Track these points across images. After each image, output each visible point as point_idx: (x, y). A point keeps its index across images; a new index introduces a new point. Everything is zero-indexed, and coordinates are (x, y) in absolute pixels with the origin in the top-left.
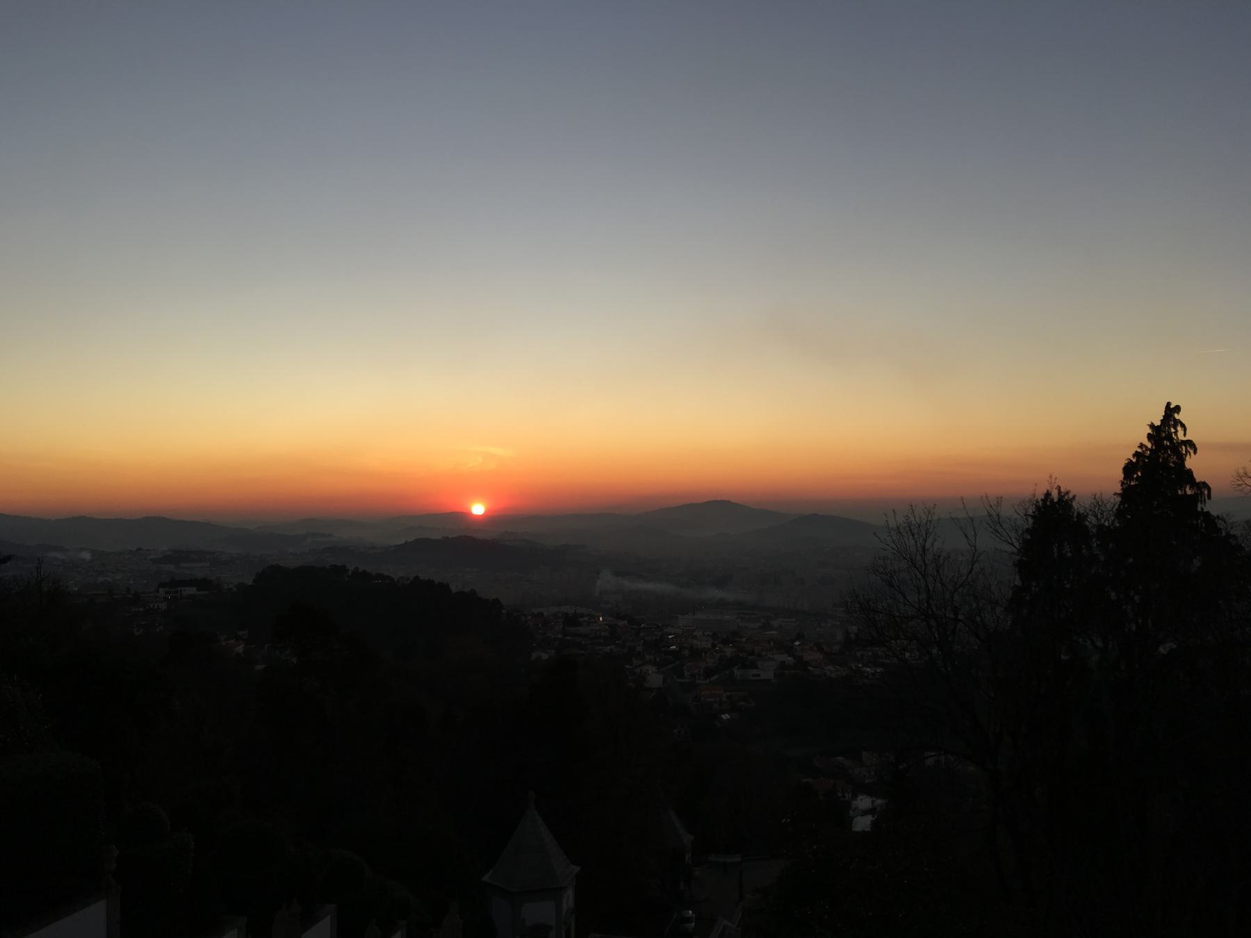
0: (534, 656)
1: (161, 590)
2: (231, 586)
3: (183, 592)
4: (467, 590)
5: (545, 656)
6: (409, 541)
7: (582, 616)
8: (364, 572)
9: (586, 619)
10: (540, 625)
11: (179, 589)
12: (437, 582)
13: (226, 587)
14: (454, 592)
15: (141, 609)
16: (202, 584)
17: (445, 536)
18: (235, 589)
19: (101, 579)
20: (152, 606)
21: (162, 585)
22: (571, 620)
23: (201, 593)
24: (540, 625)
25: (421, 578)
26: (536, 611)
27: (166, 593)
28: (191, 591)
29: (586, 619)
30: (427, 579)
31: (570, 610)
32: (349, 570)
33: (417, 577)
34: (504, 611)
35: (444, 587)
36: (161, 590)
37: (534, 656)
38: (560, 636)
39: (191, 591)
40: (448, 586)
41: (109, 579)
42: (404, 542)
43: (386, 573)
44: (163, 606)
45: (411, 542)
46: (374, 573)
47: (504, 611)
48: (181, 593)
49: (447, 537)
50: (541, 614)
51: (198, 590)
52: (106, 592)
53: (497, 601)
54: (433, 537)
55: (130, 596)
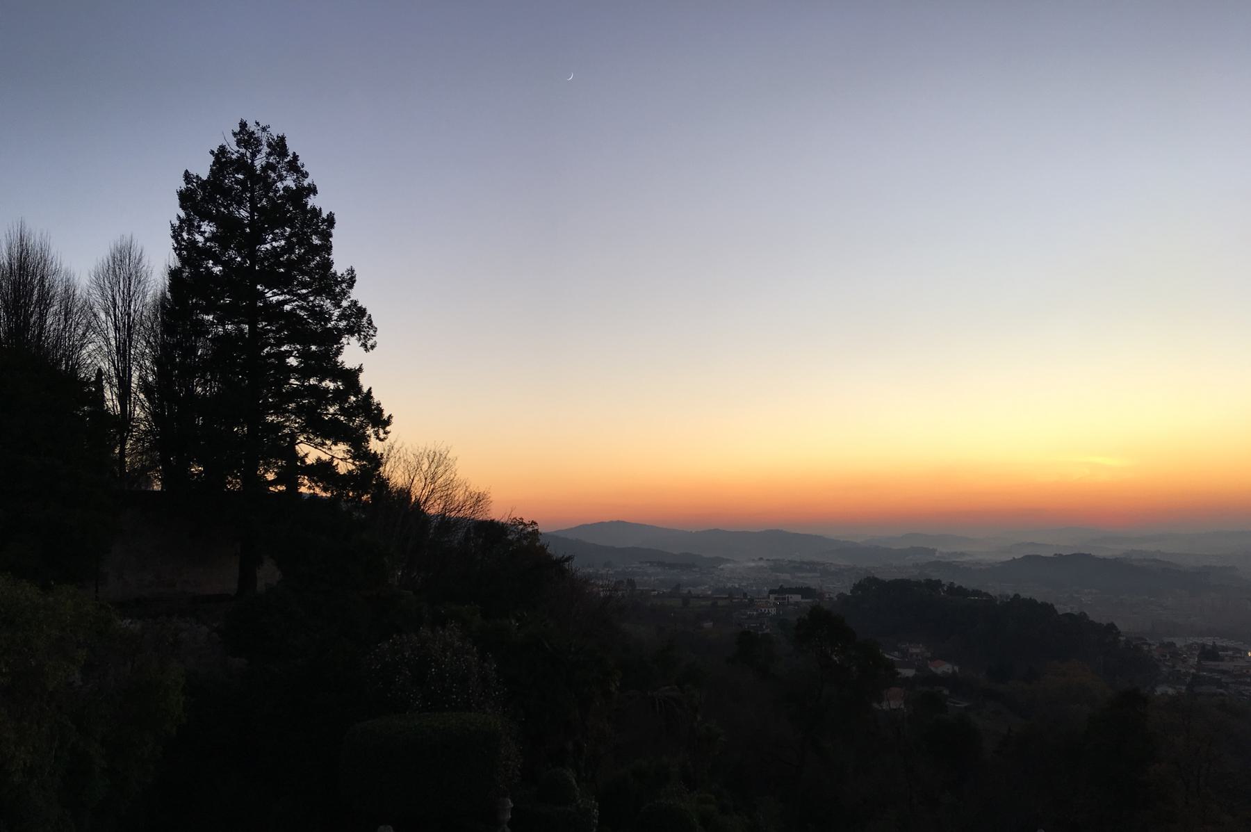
0: (1159, 690)
1: (771, 595)
2: (832, 595)
3: (790, 600)
4: (1076, 611)
5: (1171, 691)
6: (1016, 557)
7: (1225, 649)
8: (960, 587)
9: (1230, 653)
10: (1168, 656)
11: (787, 596)
12: (1039, 602)
13: (827, 596)
14: (1060, 613)
15: (755, 613)
16: (806, 592)
17: (1058, 553)
18: (836, 599)
19: (729, 585)
20: (763, 610)
21: (772, 592)
22: (1210, 654)
23: (803, 601)
24: (1168, 656)
25: (1022, 597)
26: (1167, 640)
27: (776, 599)
28: (797, 598)
29: (1230, 653)
30: (1028, 598)
31: (1209, 641)
32: (944, 584)
33: (1017, 596)
34: (1122, 638)
35: (1048, 608)
36: (771, 595)
37: (1159, 690)
38: (1193, 671)
39: (797, 598)
40: (1052, 605)
41: (737, 586)
42: (1011, 558)
43: (984, 590)
44: (773, 611)
45: (1020, 559)
46: (971, 590)
47: (1122, 638)
48: (788, 602)
49: (1060, 555)
50: (1173, 644)
51: (802, 598)
52: (727, 596)
53: (1111, 627)
54: (1043, 555)
55: (746, 600)
